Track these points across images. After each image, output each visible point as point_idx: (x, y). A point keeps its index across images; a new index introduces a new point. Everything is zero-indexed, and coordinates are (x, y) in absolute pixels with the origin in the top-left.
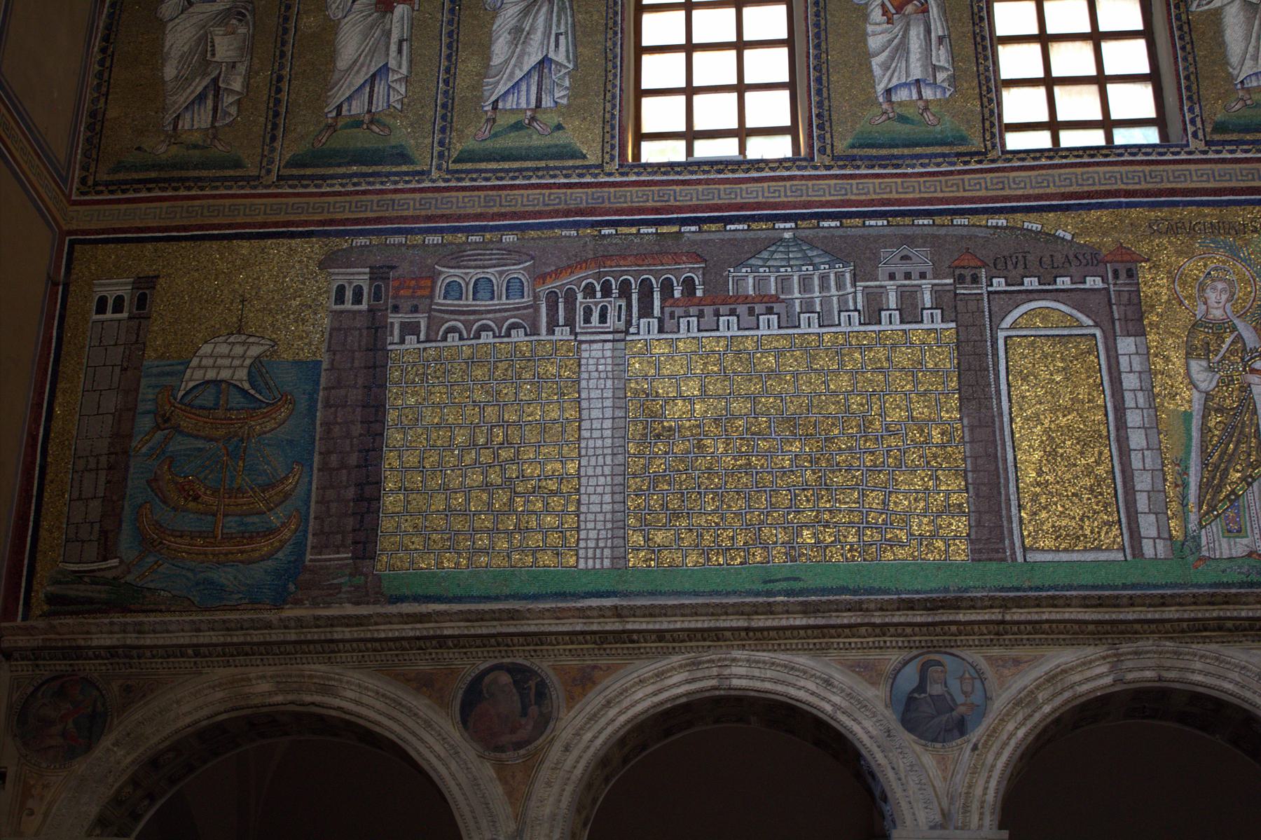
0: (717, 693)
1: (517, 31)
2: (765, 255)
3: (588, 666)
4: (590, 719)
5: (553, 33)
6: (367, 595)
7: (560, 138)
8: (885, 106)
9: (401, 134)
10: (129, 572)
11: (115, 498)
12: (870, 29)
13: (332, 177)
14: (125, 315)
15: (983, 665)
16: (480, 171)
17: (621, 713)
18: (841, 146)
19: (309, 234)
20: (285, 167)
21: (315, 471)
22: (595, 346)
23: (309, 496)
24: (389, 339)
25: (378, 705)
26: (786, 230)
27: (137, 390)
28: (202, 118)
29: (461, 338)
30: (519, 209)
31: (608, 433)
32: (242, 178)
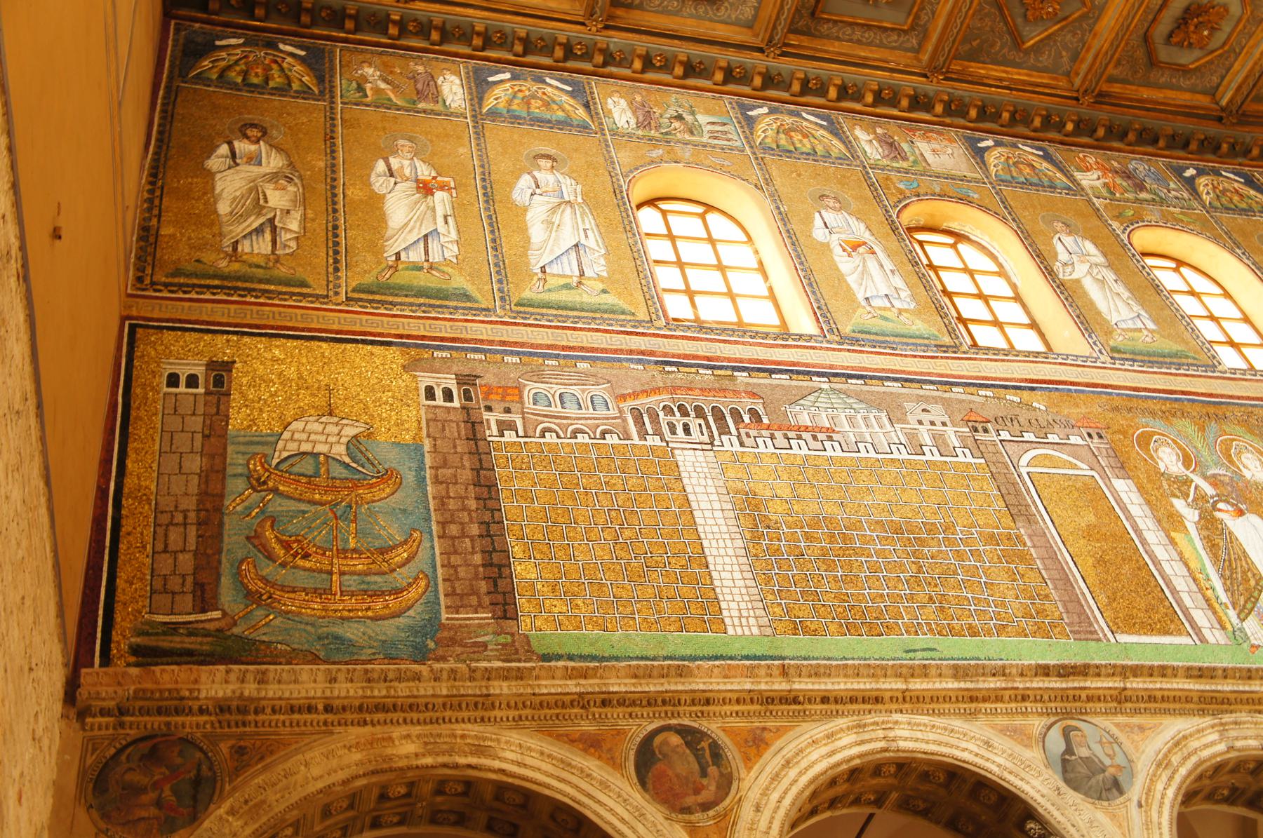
0: (887, 755)
1: (549, 223)
2: (810, 398)
3: (758, 728)
4: (773, 779)
5: (581, 227)
6: (517, 652)
7: (610, 299)
8: (868, 308)
9: (459, 282)
10: (235, 624)
11: (209, 551)
12: (836, 258)
13: (401, 304)
14: (201, 390)
15: (1115, 730)
16: (542, 315)
17: (801, 774)
18: (847, 329)
19: (389, 344)
20: (354, 290)
21: (436, 539)
22: (686, 452)
23: (434, 560)
24: (488, 433)
25: (545, 766)
26: (824, 384)
27: (224, 455)
28: (263, 246)
29: (558, 437)
30: (584, 344)
31: (721, 522)
32: (311, 295)
